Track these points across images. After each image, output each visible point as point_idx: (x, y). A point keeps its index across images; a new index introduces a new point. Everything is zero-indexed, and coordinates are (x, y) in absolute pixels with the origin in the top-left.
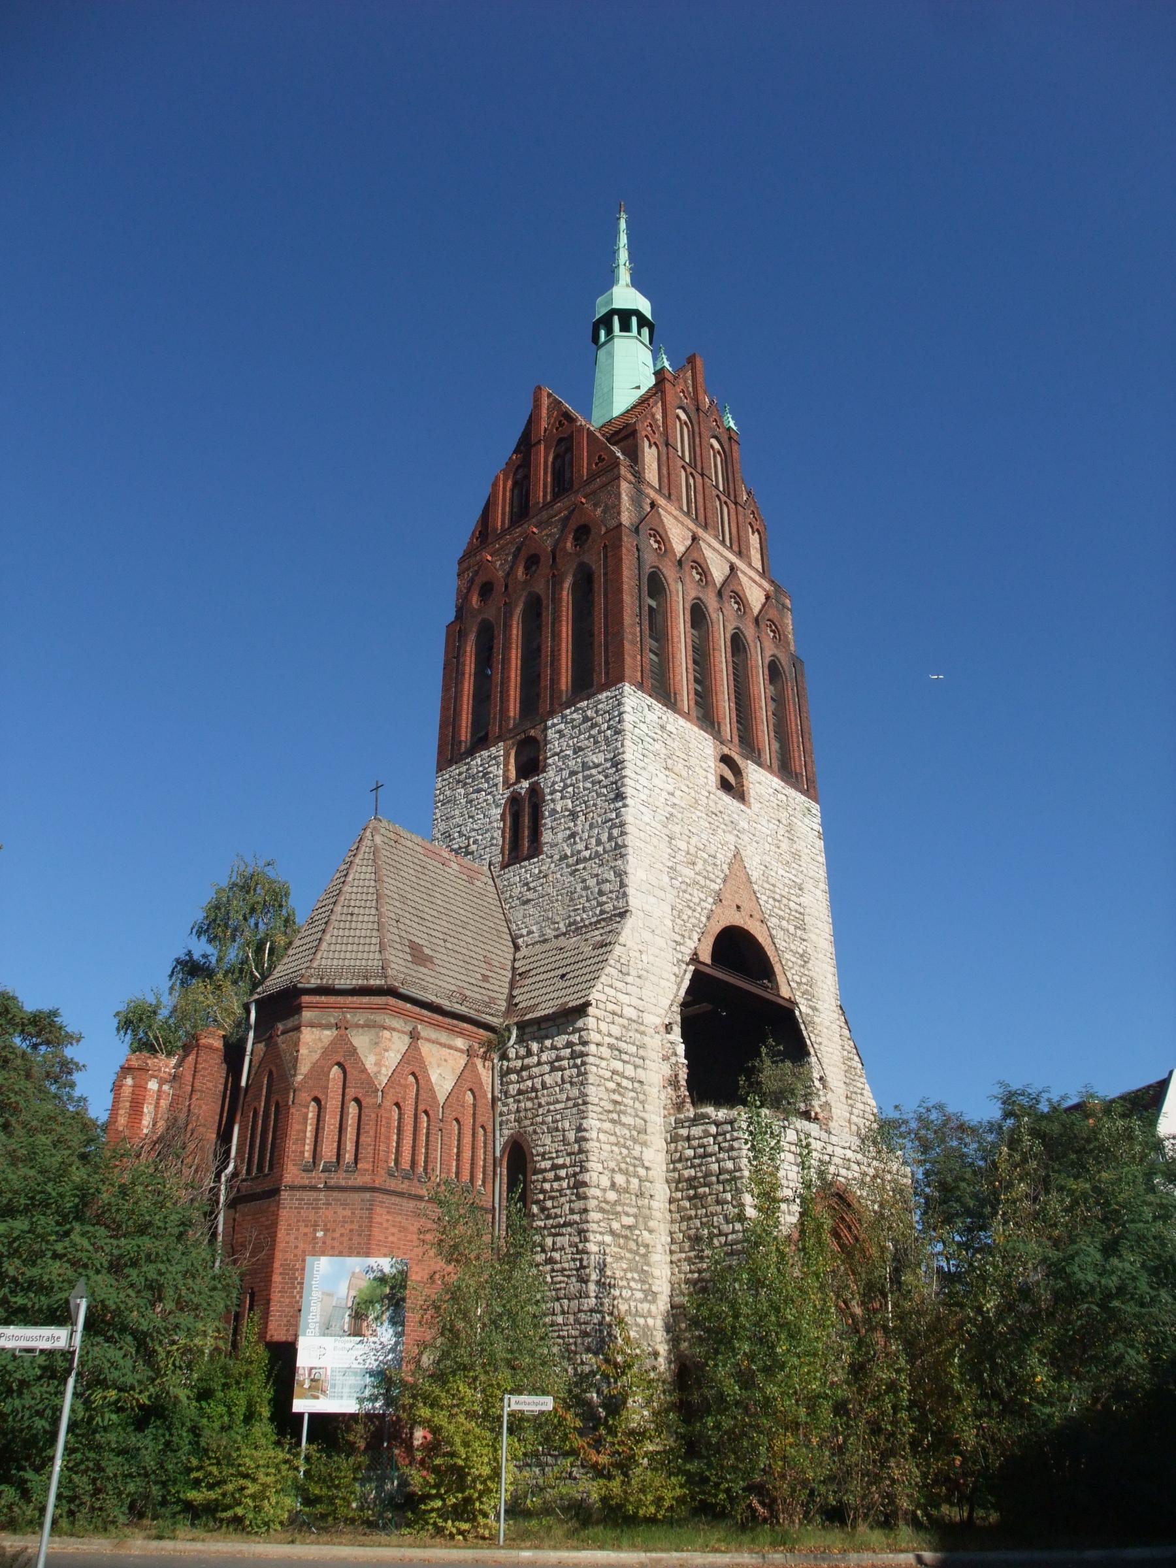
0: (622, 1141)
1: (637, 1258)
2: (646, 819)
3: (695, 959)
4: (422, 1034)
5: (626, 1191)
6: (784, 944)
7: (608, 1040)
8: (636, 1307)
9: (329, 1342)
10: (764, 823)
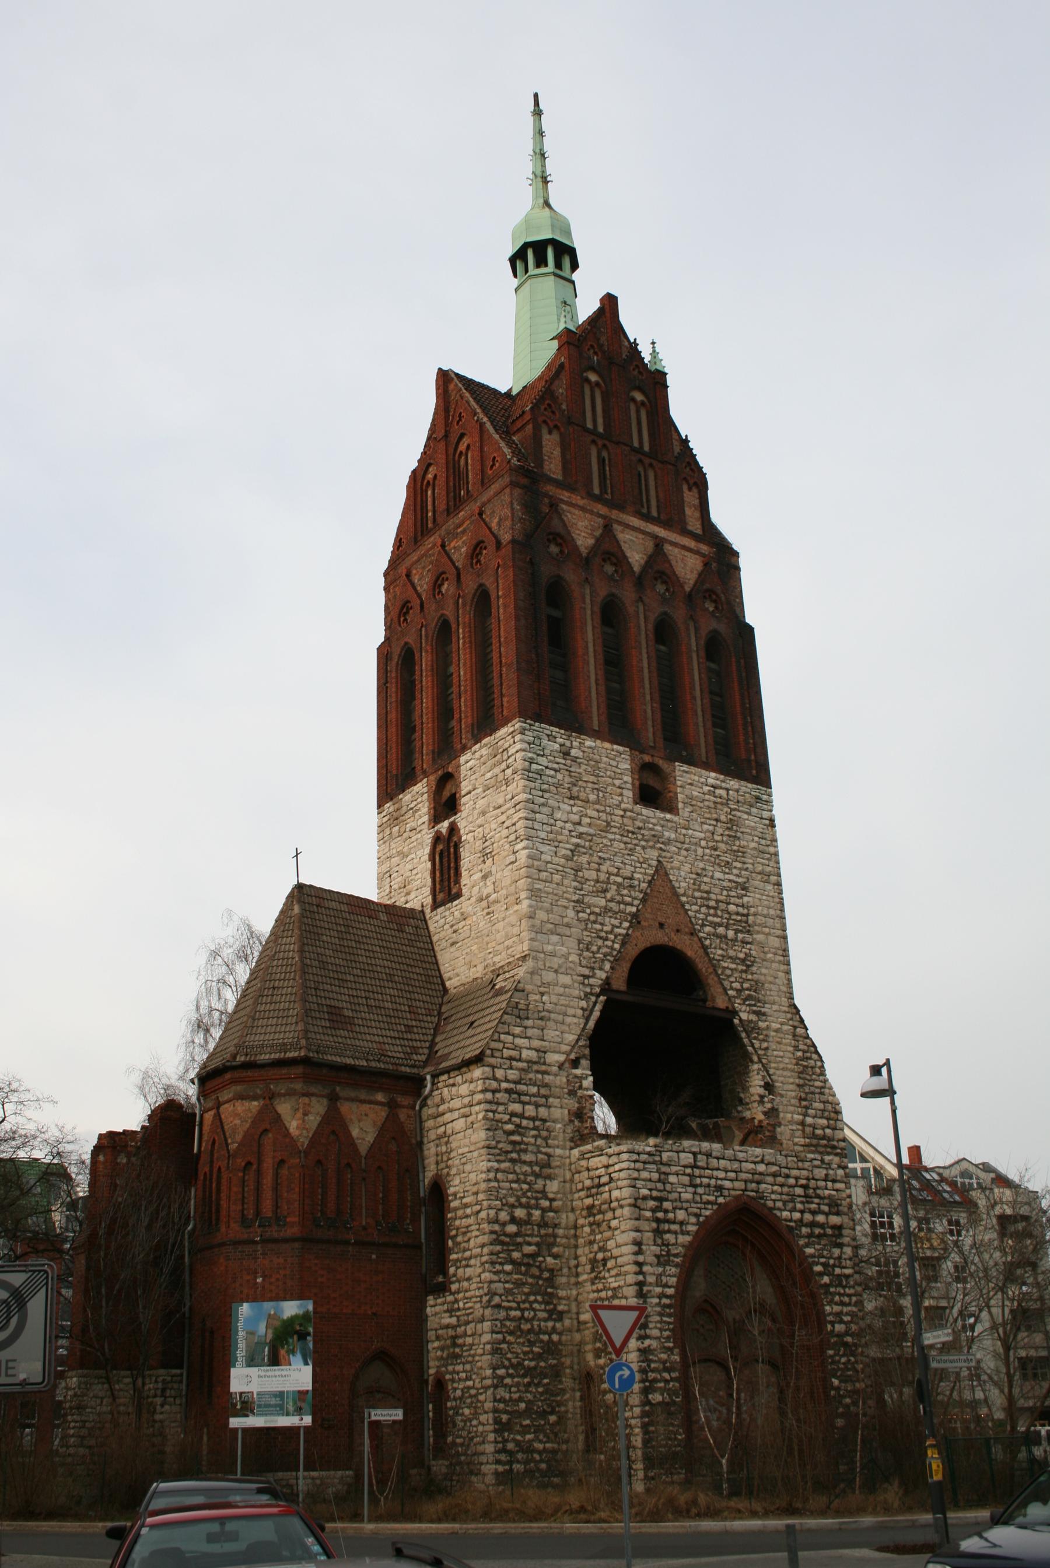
0: (522, 1177)
1: (541, 1282)
2: (546, 857)
3: (606, 987)
4: (341, 1094)
5: (528, 1222)
6: (720, 952)
7: (504, 1085)
8: (539, 1326)
9: (253, 1371)
10: (697, 827)
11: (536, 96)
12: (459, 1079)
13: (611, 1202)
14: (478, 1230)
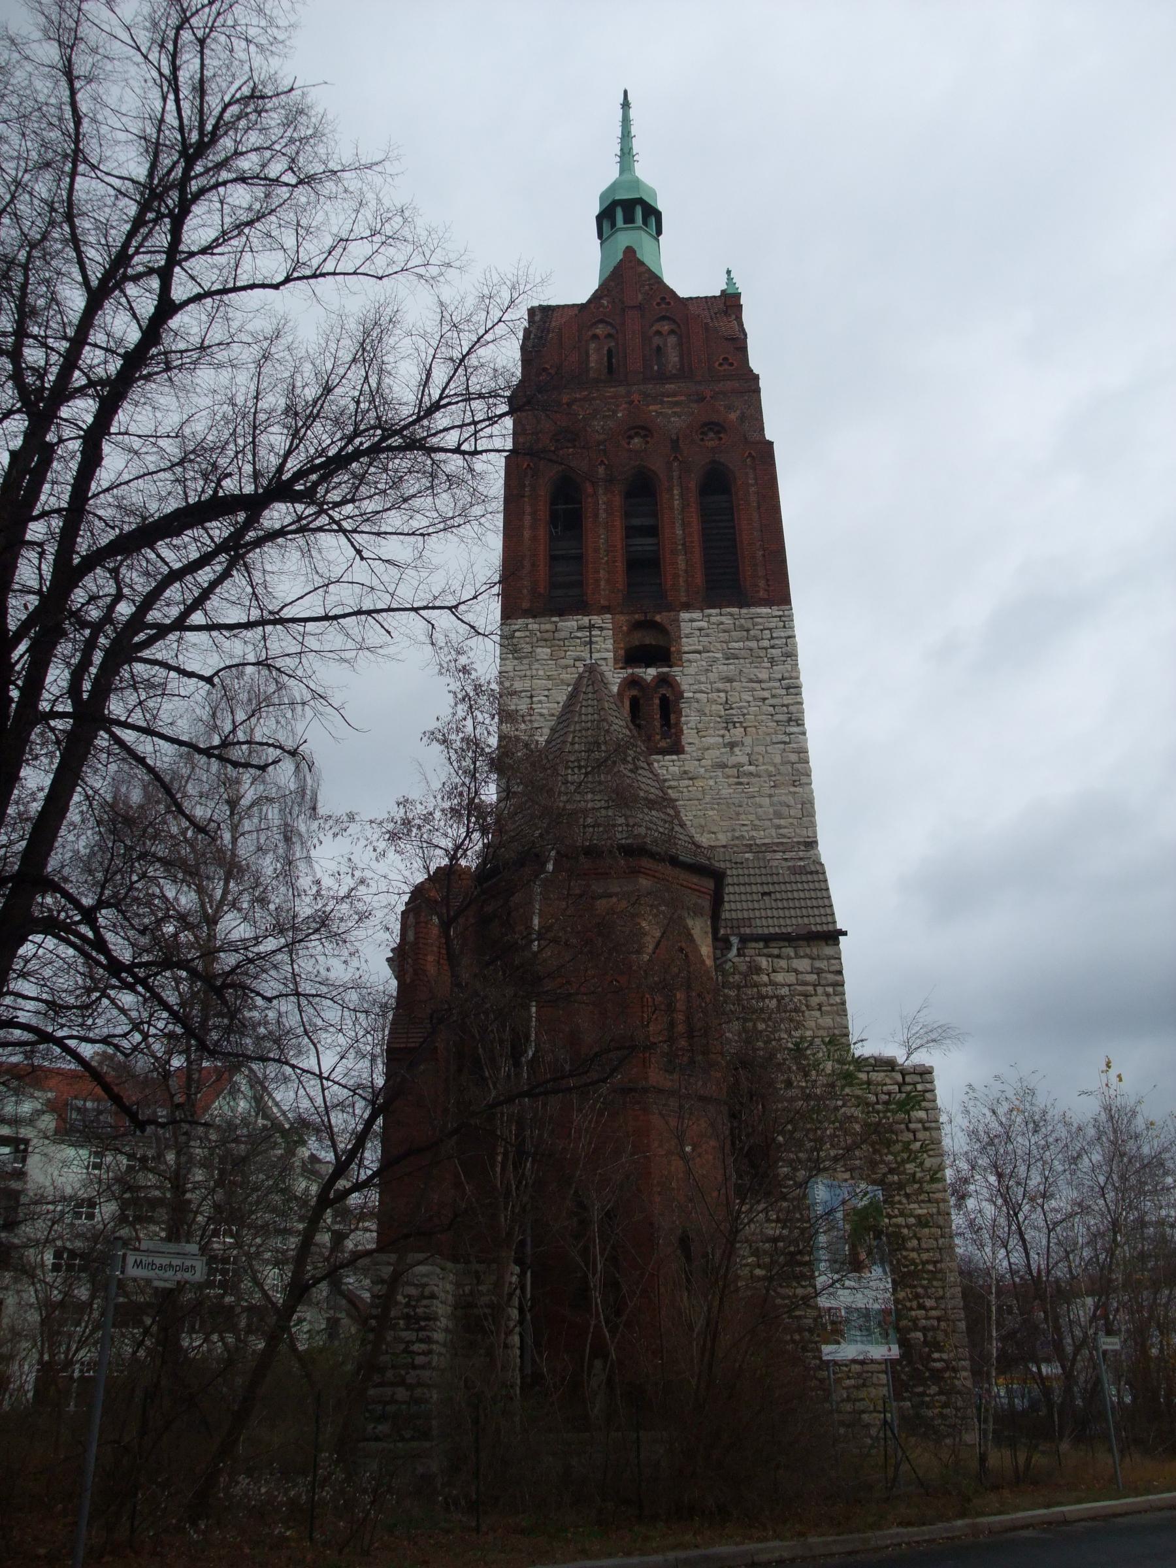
11: (626, 92)
12: (791, 952)
13: (910, 1122)
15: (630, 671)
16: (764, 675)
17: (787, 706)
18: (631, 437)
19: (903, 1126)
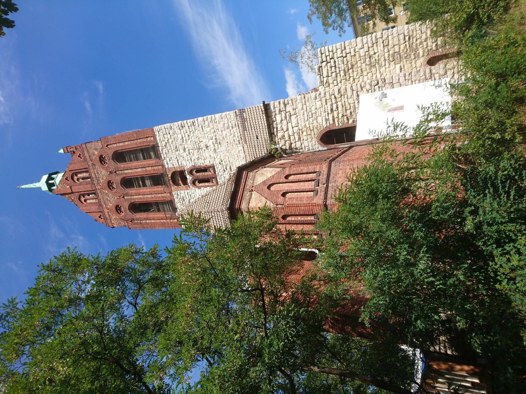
14: (344, 95)
15: (190, 184)
16: (180, 137)
17: (189, 127)
18: (113, 188)
19: (345, 59)
